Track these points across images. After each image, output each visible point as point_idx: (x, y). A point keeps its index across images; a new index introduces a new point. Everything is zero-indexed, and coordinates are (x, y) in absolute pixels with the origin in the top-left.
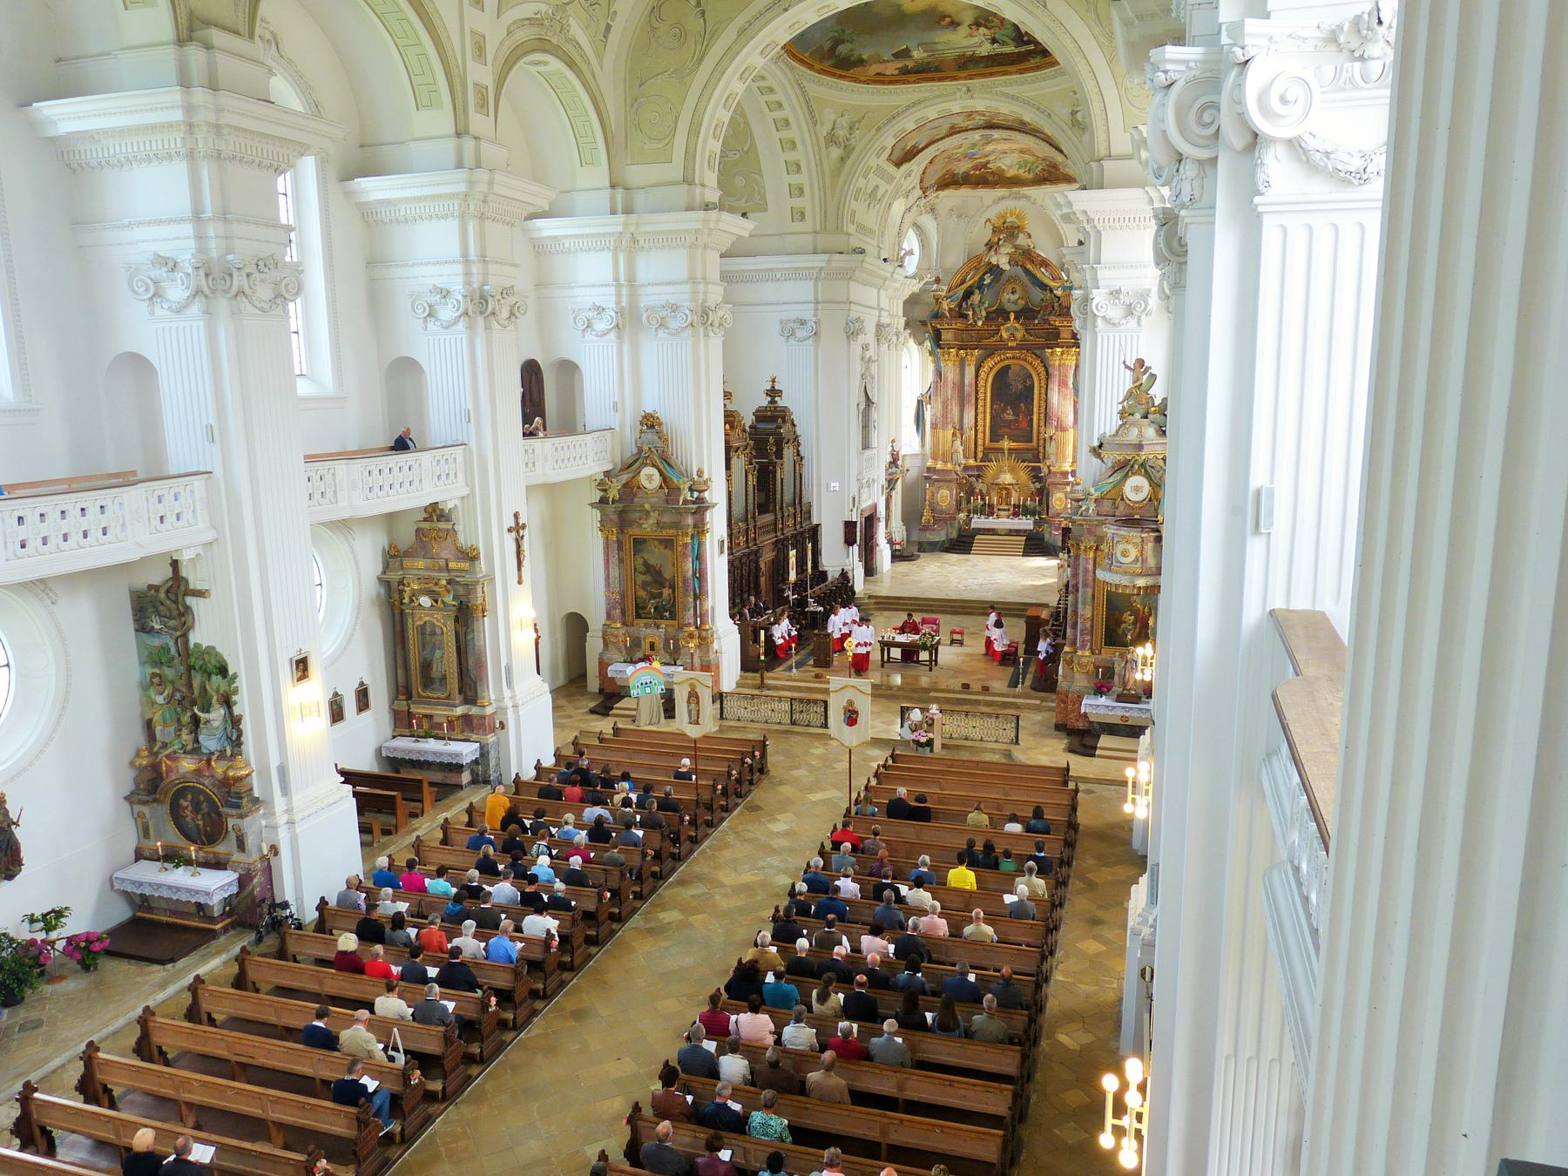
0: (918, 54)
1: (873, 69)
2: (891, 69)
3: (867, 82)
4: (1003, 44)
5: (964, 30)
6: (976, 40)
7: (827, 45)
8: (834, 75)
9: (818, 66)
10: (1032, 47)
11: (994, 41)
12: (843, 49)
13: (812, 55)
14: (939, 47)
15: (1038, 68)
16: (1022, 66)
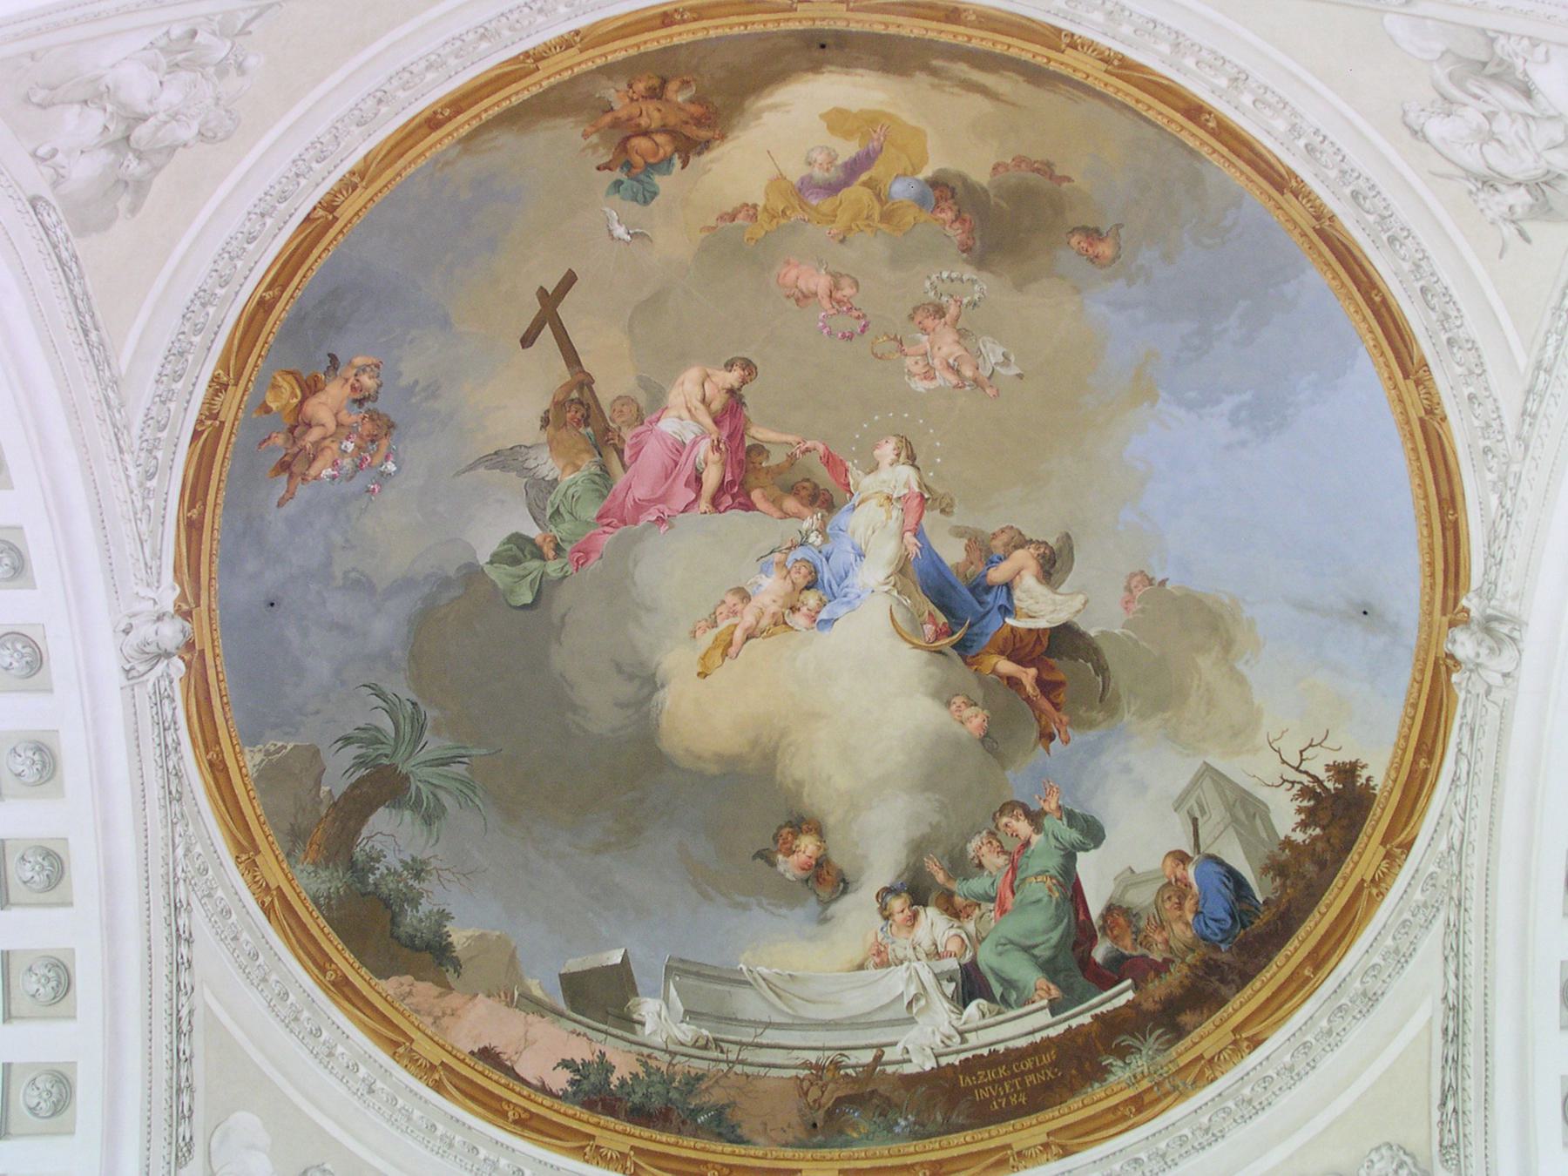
0: (660, 1018)
1: (480, 1022)
2: (548, 1050)
3: (442, 1078)
4: (1007, 997)
5: (857, 917)
6: (896, 982)
7: (336, 783)
8: (318, 962)
9: (273, 870)
10: (1122, 996)
11: (971, 985)
12: (389, 835)
13: (272, 775)
14: (749, 1004)
15: (1140, 1106)
16: (1074, 1111)
